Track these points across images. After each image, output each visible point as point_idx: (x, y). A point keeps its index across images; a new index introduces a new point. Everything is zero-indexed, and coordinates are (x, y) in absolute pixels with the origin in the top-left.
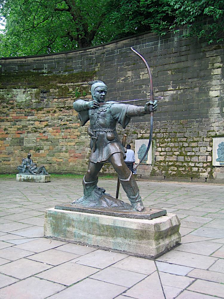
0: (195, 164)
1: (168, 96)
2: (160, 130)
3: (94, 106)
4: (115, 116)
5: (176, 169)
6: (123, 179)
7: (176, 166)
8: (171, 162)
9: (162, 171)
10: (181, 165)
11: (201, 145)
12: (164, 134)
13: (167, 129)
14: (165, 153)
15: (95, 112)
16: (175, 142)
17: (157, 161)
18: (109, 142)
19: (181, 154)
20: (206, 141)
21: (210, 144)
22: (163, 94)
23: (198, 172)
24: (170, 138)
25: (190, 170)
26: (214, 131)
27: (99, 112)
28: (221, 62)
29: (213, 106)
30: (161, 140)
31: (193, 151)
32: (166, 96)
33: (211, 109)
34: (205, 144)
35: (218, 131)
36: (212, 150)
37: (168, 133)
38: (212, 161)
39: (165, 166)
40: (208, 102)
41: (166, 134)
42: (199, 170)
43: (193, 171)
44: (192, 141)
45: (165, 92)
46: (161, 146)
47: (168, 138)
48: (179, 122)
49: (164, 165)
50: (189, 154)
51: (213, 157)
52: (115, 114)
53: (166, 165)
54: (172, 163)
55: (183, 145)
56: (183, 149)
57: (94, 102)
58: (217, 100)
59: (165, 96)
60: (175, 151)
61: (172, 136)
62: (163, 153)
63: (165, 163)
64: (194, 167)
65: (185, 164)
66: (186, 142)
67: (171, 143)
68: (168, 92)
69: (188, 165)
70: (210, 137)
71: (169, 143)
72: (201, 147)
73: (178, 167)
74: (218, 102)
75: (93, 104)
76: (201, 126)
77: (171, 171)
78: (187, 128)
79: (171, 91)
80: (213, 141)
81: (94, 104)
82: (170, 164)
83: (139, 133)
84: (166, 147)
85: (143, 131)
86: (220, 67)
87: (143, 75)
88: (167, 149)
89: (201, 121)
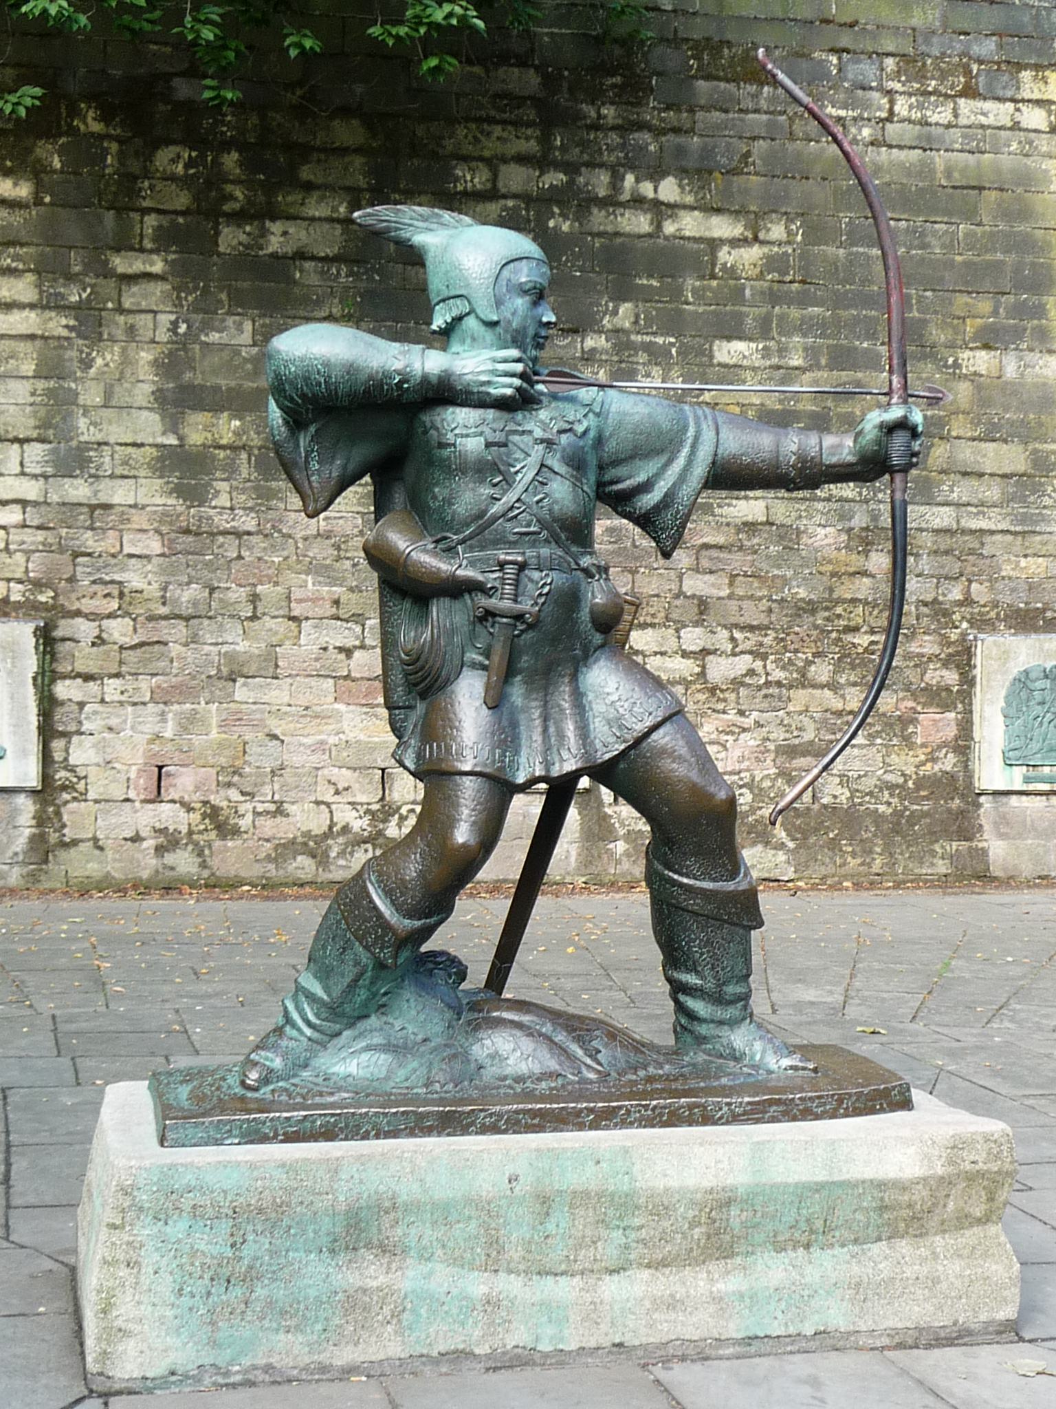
3: (518, 389)
6: (714, 880)
18: (598, 638)
27: (547, 436)
52: (616, 463)
57: (518, 360)
81: (523, 376)
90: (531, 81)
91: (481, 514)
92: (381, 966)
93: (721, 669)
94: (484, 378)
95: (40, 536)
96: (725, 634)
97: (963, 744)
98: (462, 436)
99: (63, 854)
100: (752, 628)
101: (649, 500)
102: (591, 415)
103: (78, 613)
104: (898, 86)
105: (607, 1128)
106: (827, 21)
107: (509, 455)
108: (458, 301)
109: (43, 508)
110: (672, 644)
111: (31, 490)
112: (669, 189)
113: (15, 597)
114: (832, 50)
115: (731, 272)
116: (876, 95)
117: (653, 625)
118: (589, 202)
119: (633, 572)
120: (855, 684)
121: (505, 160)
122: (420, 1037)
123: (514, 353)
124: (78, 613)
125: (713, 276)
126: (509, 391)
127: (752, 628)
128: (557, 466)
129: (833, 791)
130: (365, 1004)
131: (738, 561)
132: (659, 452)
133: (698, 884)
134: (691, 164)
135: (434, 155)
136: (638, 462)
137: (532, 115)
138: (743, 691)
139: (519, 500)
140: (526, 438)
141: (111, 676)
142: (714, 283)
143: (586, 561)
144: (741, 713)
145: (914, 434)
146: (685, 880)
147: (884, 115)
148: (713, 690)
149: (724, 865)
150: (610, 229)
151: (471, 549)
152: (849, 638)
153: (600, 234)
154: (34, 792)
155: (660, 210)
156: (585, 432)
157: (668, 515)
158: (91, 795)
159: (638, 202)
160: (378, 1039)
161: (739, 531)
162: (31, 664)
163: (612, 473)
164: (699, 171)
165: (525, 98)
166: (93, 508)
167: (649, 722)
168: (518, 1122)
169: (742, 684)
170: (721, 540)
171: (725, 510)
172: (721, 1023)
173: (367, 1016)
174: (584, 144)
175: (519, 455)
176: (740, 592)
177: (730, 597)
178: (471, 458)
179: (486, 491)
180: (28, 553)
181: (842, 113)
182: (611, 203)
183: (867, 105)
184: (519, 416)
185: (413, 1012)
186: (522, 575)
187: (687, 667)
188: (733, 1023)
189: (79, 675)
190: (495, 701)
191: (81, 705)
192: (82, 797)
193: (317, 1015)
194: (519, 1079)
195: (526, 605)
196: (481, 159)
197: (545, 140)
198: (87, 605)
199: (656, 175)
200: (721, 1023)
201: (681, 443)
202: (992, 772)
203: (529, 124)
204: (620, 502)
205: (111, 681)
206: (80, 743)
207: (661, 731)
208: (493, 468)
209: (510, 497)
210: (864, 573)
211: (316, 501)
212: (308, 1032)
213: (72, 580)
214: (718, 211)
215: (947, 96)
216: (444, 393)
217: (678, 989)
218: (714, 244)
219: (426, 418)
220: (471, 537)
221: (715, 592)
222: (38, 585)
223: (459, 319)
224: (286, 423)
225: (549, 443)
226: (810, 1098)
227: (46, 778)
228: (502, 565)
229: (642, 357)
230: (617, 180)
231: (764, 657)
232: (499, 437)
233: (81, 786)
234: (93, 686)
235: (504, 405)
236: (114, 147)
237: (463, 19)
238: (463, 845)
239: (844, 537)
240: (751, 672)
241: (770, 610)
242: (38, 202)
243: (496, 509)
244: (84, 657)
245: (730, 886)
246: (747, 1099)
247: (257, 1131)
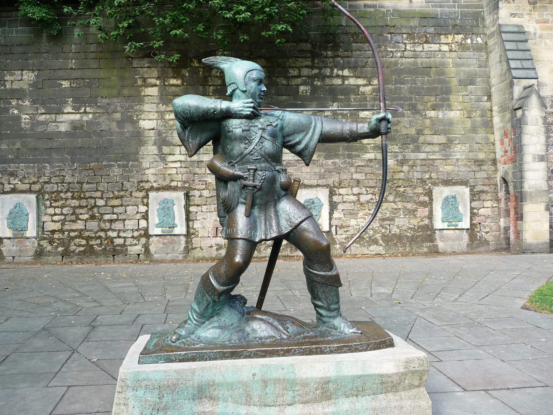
0: (118, 233)
1: (64, 122)
2: (51, 178)
3: (252, 112)
4: (291, 138)
5: (84, 242)
6: (324, 272)
7: (83, 238)
8: (74, 231)
9: (57, 247)
10: (94, 236)
11: (129, 203)
12: (59, 185)
13: (64, 176)
14: (63, 217)
15: (252, 126)
16: (80, 198)
17: (47, 231)
18: (283, 193)
19: (93, 217)
20: (136, 198)
21: (143, 202)
22: (54, 119)
23: (124, 245)
24: (71, 192)
25: (110, 243)
26: (148, 181)
27: (262, 127)
28: (158, 78)
29: (145, 143)
30: (53, 196)
31: (115, 212)
32: (61, 122)
33: (142, 148)
35: (155, 182)
36: (147, 211)
37: (65, 183)
38: (148, 227)
39: (61, 239)
40: (138, 136)
41: (63, 186)
42: (125, 241)
43: (115, 244)
44: (112, 196)
45: (58, 116)
46: (53, 205)
47: (66, 192)
48: (86, 166)
49: (61, 236)
50: (107, 217)
51: (149, 220)
52: (289, 135)
53: (65, 237)
54: (76, 233)
55: (95, 203)
56: (95, 210)
57: (252, 103)
58: (153, 135)
59: (59, 122)
60: (81, 214)
61: (74, 189)
62: (57, 217)
63: (63, 234)
64: (116, 238)
65: (102, 234)
66: (102, 198)
67: (74, 201)
68: (64, 116)
69: (106, 234)
71: (70, 201)
72: (128, 205)
73: (88, 239)
74: (153, 138)
75: (250, 107)
76: (126, 173)
77: (75, 247)
78: (101, 176)
79: (70, 115)
80: (150, 197)
81: (253, 108)
82: (72, 234)
83: (6, 182)
84: (62, 207)
85: (15, 179)
86: (156, 85)
87: (12, 81)
88: (65, 211)
89: (127, 166)
90: (309, 46)
91: (242, 154)
92: (214, 301)
93: (363, 198)
94: (240, 109)
95: (185, 170)
96: (364, 189)
97: (430, 216)
98: (235, 128)
99: (193, 251)
100: (372, 187)
101: (300, 147)
102: (279, 120)
103: (195, 189)
104: (407, 42)
105: (288, 356)
106: (387, 26)
107: (250, 134)
108: (233, 85)
109: (186, 163)
110: (350, 192)
111: (183, 158)
112: (346, 72)
113: (179, 186)
114: (389, 33)
115: (363, 93)
116: (401, 44)
117: (345, 187)
118: (324, 77)
119: (339, 173)
120: (400, 201)
121: (302, 67)
122: (230, 324)
123: (251, 100)
124: (195, 189)
125: (359, 95)
126: (249, 113)
127: (372, 187)
128: (266, 137)
129: (395, 230)
130: (212, 313)
131: (367, 170)
132: (303, 131)
133: (319, 273)
134: (352, 65)
135: (284, 67)
136: (296, 135)
137: (309, 55)
138: (370, 204)
139: (254, 148)
140: (256, 128)
142: (359, 96)
143: (278, 168)
144: (369, 210)
145: (388, 121)
146: (315, 272)
147: (403, 49)
148: (361, 204)
149: (327, 267)
150: (330, 83)
151: (239, 165)
152: (398, 189)
153: (328, 85)
154: (185, 235)
155: (344, 78)
156: (276, 126)
157: (307, 152)
158: (199, 236)
159: (338, 76)
160: (216, 324)
161: (367, 161)
162: (183, 203)
163: (287, 139)
164: (354, 67)
165: (307, 51)
166: (198, 162)
167: (300, 220)
168: (257, 354)
169: (369, 202)
170: (363, 164)
171: (364, 156)
172: (330, 317)
173: (213, 317)
174: (323, 62)
175: (254, 134)
176: (368, 178)
177: (365, 179)
178: (238, 135)
179: (243, 146)
180: (182, 174)
181: (392, 50)
182: (331, 77)
183: (399, 47)
184: (253, 121)
185: (228, 315)
186: (256, 173)
187: (354, 198)
188: (334, 317)
189: (196, 205)
190: (248, 214)
191: (197, 213)
192: (197, 236)
193: (197, 317)
194: (261, 338)
195: (257, 183)
196: (296, 67)
197: (313, 61)
198: (197, 187)
199: (342, 69)
200: (330, 317)
201: (310, 128)
202: (438, 224)
203: (308, 58)
204: (291, 148)
207: (304, 223)
208: (245, 139)
209: (251, 148)
210: (402, 172)
211: (191, 152)
212: (195, 322)
213: (193, 181)
214: (359, 77)
215: (421, 43)
216: (228, 115)
217: (316, 306)
218: (358, 86)
219: (224, 123)
220: (239, 161)
221: (361, 178)
222: (185, 182)
223: (234, 91)
224: (181, 127)
225: (263, 129)
226: (358, 345)
227: (188, 231)
228: (249, 170)
229: (340, 117)
230: (332, 70)
231: (375, 195)
232: (247, 128)
233: (197, 233)
234: (199, 208)
235: (247, 117)
236: (202, 70)
237: (286, 29)
238: (238, 263)
239: (396, 162)
240: (372, 199)
241: (376, 182)
242: (183, 85)
243: (247, 151)
244: (197, 200)
245: (330, 273)
246: (336, 345)
247: (170, 359)
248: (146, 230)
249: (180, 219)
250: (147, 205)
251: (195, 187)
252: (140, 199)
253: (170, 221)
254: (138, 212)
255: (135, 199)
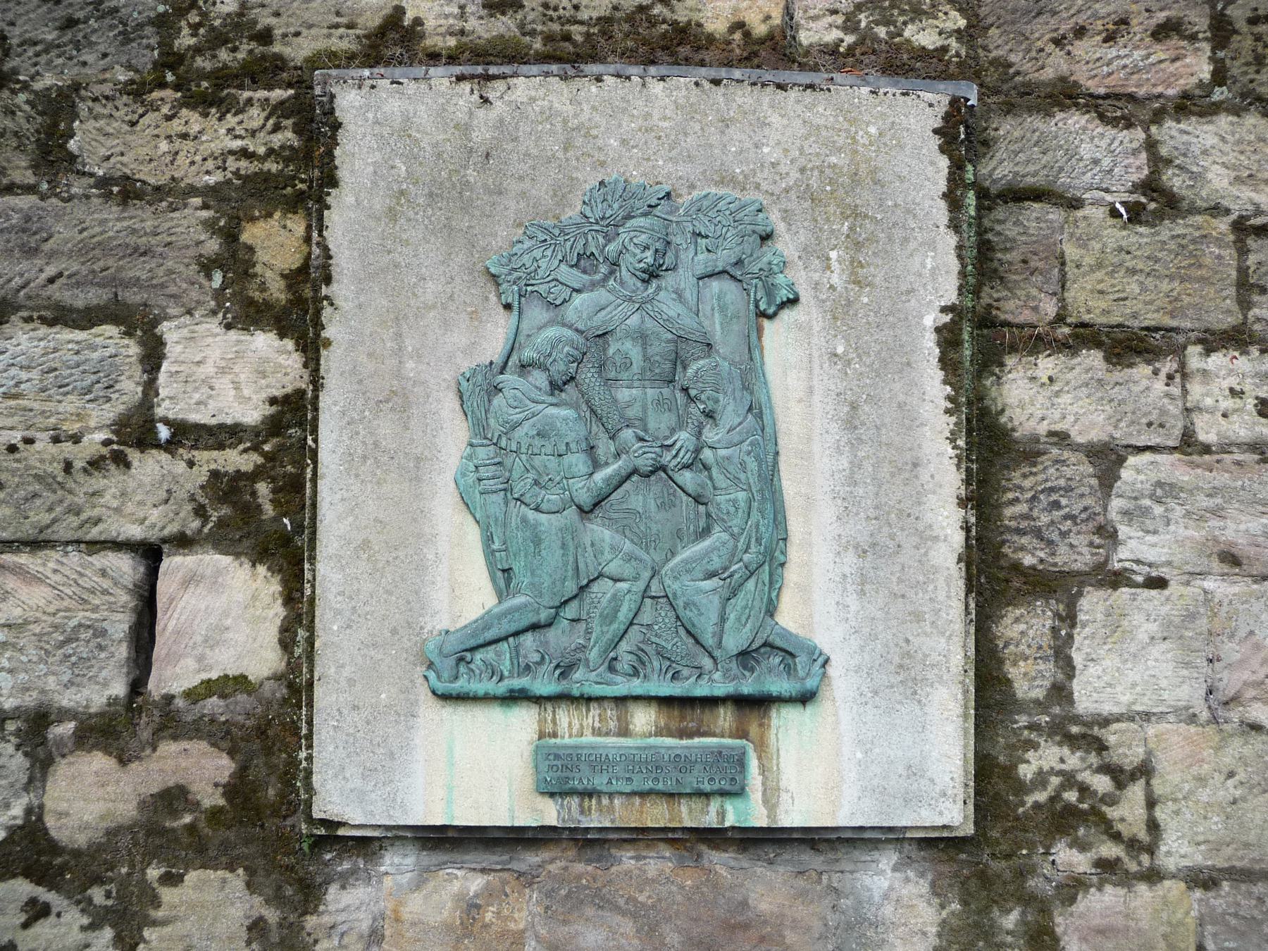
20: (125, 190)
21: (235, 261)
34: (83, 250)
36: (295, 413)
38: (297, 687)
51: (330, 573)
70: (222, 77)
80: (356, 156)
103: (1065, 95)
124: (1065, 95)
141: (1213, 341)
154: (936, 846)
158: (1177, 850)
189: (1086, 336)
191: (1107, 459)
192: (1136, 861)
198: (1095, 65)
205: (1217, 360)
206: (1115, 624)
227: (990, 778)
233: (1129, 811)
234: (1146, 383)
244: (1106, 270)
248: (271, 727)
249: (878, 550)
250: (299, 314)
251: (1055, 65)
252: (190, 225)
253: (703, 596)
254: (137, 431)
255: (111, 221)
